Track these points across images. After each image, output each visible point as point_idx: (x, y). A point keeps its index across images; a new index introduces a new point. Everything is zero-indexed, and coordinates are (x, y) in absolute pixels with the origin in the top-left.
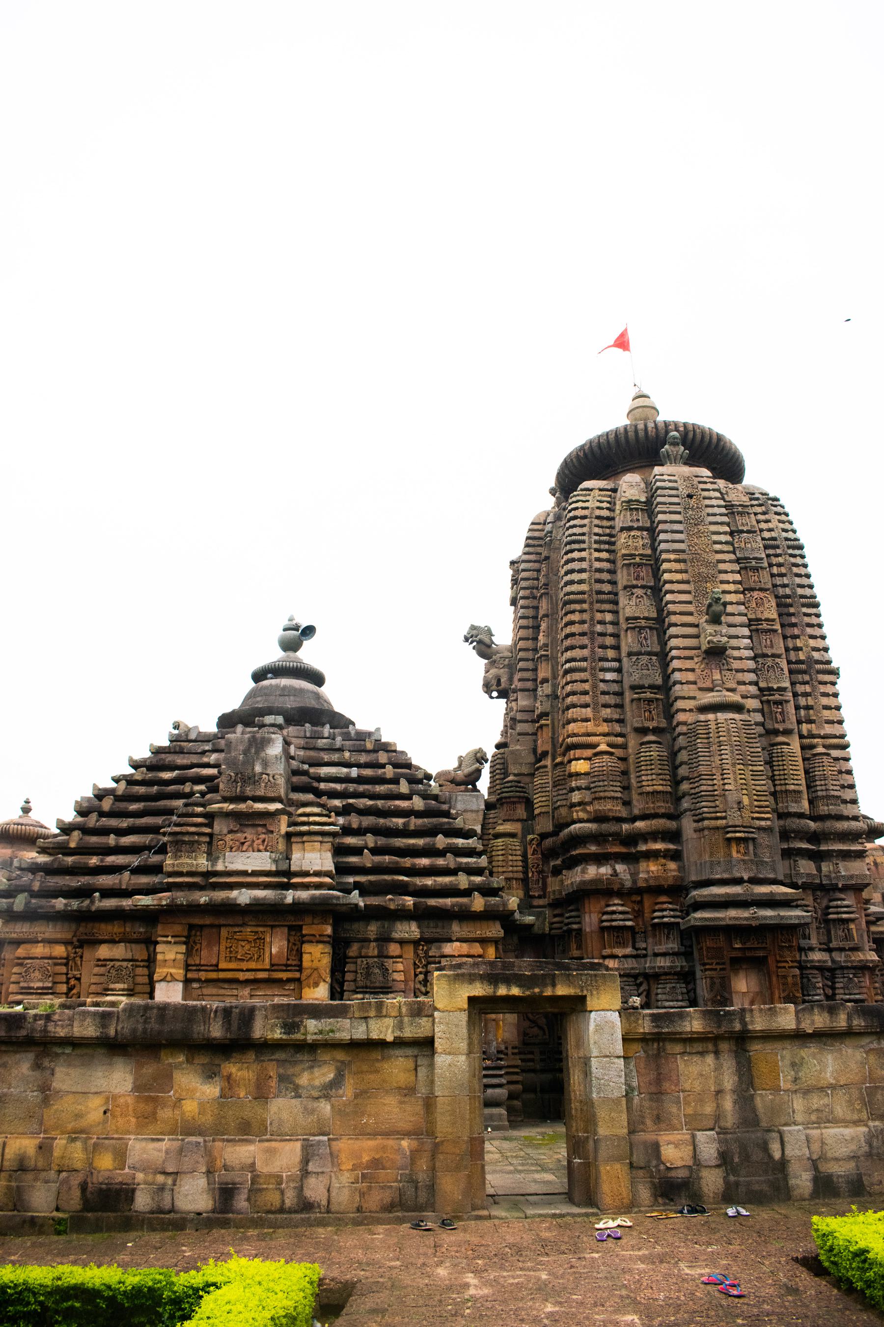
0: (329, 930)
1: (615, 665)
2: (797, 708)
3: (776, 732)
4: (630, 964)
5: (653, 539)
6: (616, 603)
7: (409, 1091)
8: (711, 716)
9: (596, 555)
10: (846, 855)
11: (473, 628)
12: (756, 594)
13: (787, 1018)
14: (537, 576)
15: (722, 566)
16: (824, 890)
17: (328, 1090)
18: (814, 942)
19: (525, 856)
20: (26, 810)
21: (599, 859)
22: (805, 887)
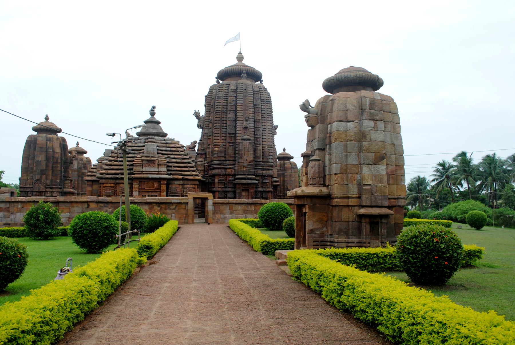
4: (224, 189)
5: (236, 99)
8: (243, 141)
14: (211, 100)
16: (263, 176)
17: (174, 209)
22: (259, 176)
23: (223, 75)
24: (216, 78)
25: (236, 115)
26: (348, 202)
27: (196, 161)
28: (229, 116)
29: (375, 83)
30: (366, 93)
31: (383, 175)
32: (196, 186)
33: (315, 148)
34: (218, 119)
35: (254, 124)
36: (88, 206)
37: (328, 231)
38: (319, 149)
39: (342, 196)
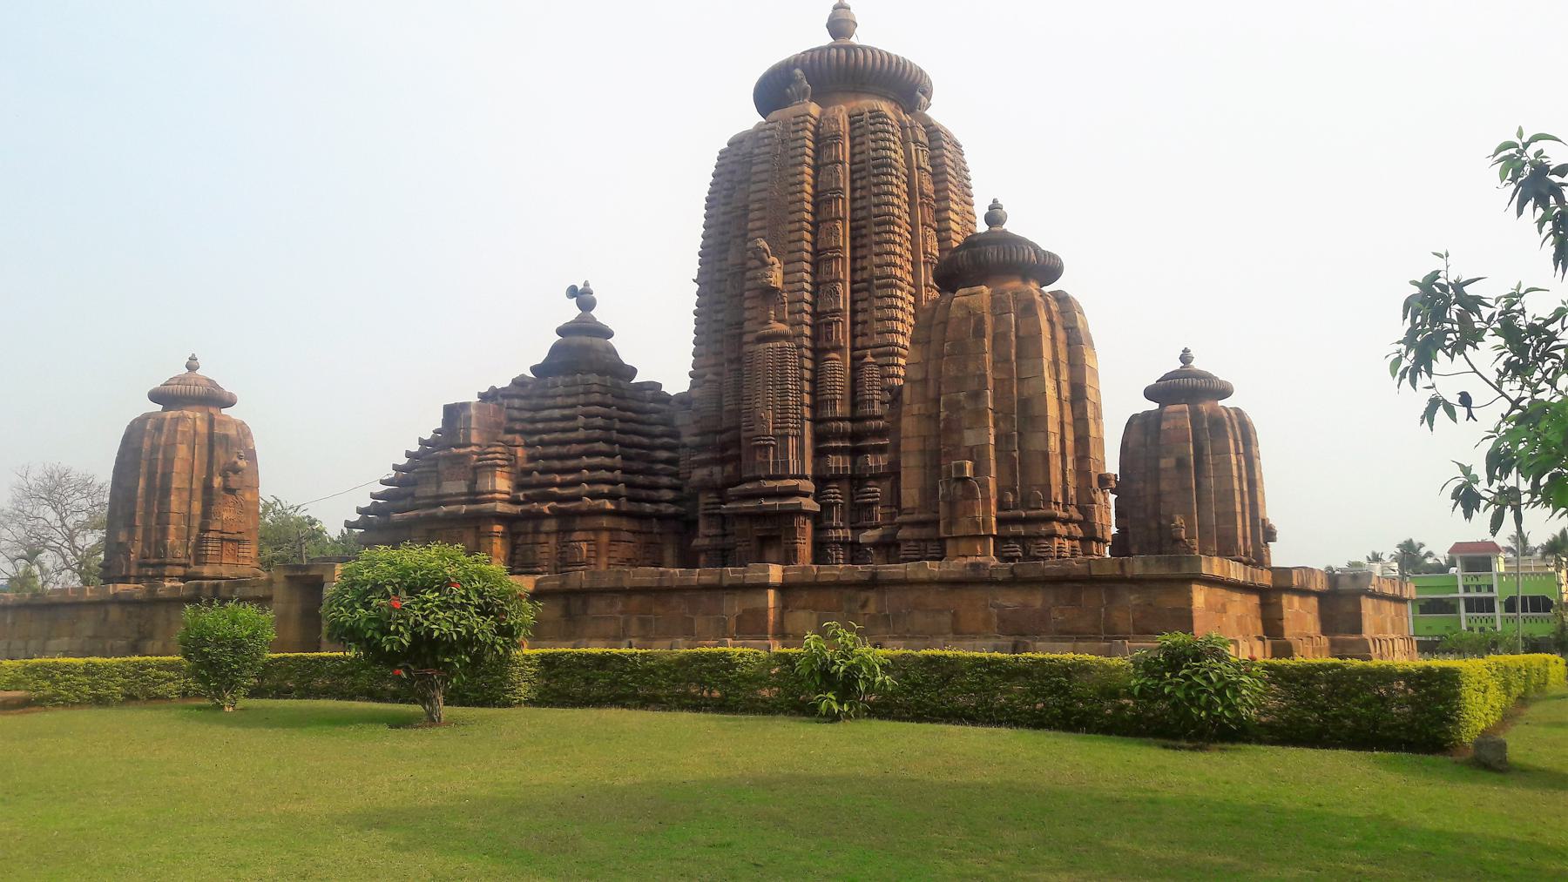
3: (827, 351)
12: (826, 226)
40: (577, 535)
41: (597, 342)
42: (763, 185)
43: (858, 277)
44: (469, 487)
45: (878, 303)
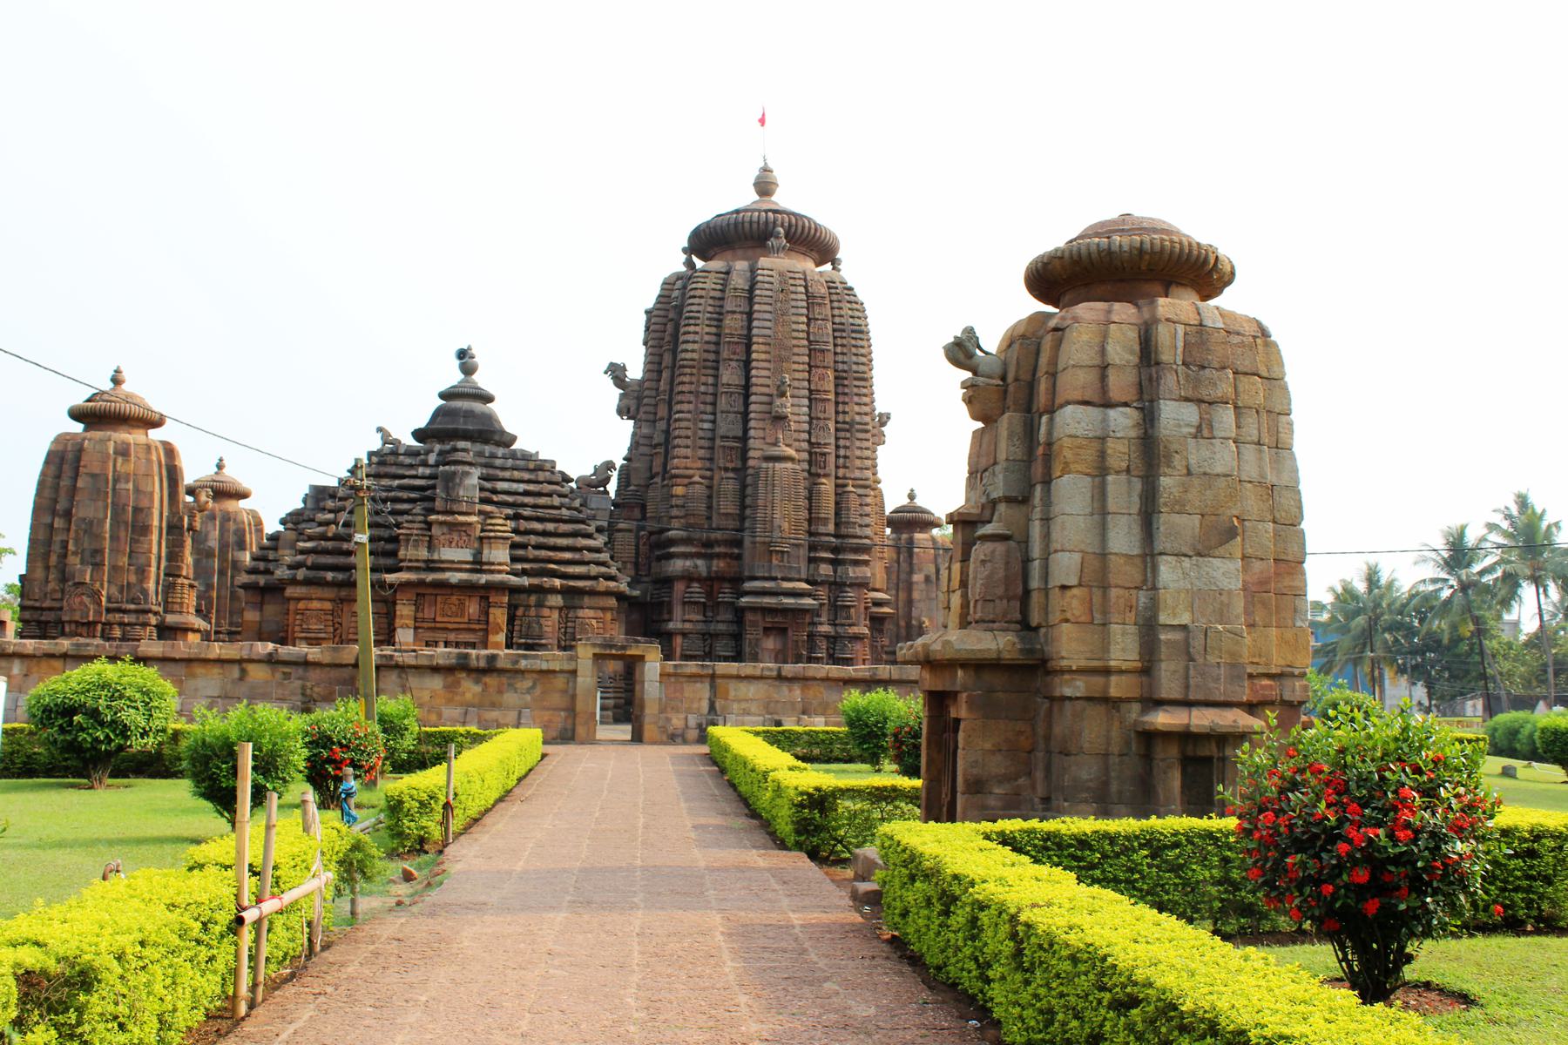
0: (506, 599)
1: (711, 417)
2: (837, 457)
3: (819, 476)
4: (700, 626)
5: (750, 320)
6: (717, 369)
7: (565, 692)
9: (707, 329)
10: (856, 563)
11: (612, 365)
12: (820, 371)
13: (733, 667)
15: (796, 350)
16: (837, 586)
17: (529, 691)
18: (824, 619)
19: (637, 546)
20: (220, 466)
21: (685, 556)
22: (822, 583)
23: (707, 241)
24: (685, 251)
25: (748, 378)
26: (1107, 686)
27: (610, 530)
28: (725, 379)
29: (1200, 272)
30: (1176, 307)
31: (1230, 592)
32: (609, 616)
33: (995, 495)
34: (686, 388)
35: (810, 407)
36: (243, 672)
37: (1033, 787)
38: (1009, 500)
39: (1083, 663)
40: (581, 613)
41: (477, 406)
42: (768, 324)
43: (841, 418)
44: (475, 556)
45: (858, 443)
